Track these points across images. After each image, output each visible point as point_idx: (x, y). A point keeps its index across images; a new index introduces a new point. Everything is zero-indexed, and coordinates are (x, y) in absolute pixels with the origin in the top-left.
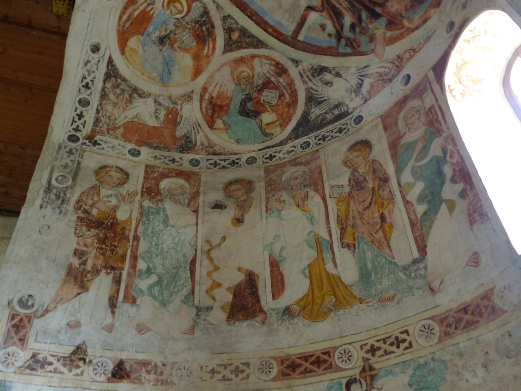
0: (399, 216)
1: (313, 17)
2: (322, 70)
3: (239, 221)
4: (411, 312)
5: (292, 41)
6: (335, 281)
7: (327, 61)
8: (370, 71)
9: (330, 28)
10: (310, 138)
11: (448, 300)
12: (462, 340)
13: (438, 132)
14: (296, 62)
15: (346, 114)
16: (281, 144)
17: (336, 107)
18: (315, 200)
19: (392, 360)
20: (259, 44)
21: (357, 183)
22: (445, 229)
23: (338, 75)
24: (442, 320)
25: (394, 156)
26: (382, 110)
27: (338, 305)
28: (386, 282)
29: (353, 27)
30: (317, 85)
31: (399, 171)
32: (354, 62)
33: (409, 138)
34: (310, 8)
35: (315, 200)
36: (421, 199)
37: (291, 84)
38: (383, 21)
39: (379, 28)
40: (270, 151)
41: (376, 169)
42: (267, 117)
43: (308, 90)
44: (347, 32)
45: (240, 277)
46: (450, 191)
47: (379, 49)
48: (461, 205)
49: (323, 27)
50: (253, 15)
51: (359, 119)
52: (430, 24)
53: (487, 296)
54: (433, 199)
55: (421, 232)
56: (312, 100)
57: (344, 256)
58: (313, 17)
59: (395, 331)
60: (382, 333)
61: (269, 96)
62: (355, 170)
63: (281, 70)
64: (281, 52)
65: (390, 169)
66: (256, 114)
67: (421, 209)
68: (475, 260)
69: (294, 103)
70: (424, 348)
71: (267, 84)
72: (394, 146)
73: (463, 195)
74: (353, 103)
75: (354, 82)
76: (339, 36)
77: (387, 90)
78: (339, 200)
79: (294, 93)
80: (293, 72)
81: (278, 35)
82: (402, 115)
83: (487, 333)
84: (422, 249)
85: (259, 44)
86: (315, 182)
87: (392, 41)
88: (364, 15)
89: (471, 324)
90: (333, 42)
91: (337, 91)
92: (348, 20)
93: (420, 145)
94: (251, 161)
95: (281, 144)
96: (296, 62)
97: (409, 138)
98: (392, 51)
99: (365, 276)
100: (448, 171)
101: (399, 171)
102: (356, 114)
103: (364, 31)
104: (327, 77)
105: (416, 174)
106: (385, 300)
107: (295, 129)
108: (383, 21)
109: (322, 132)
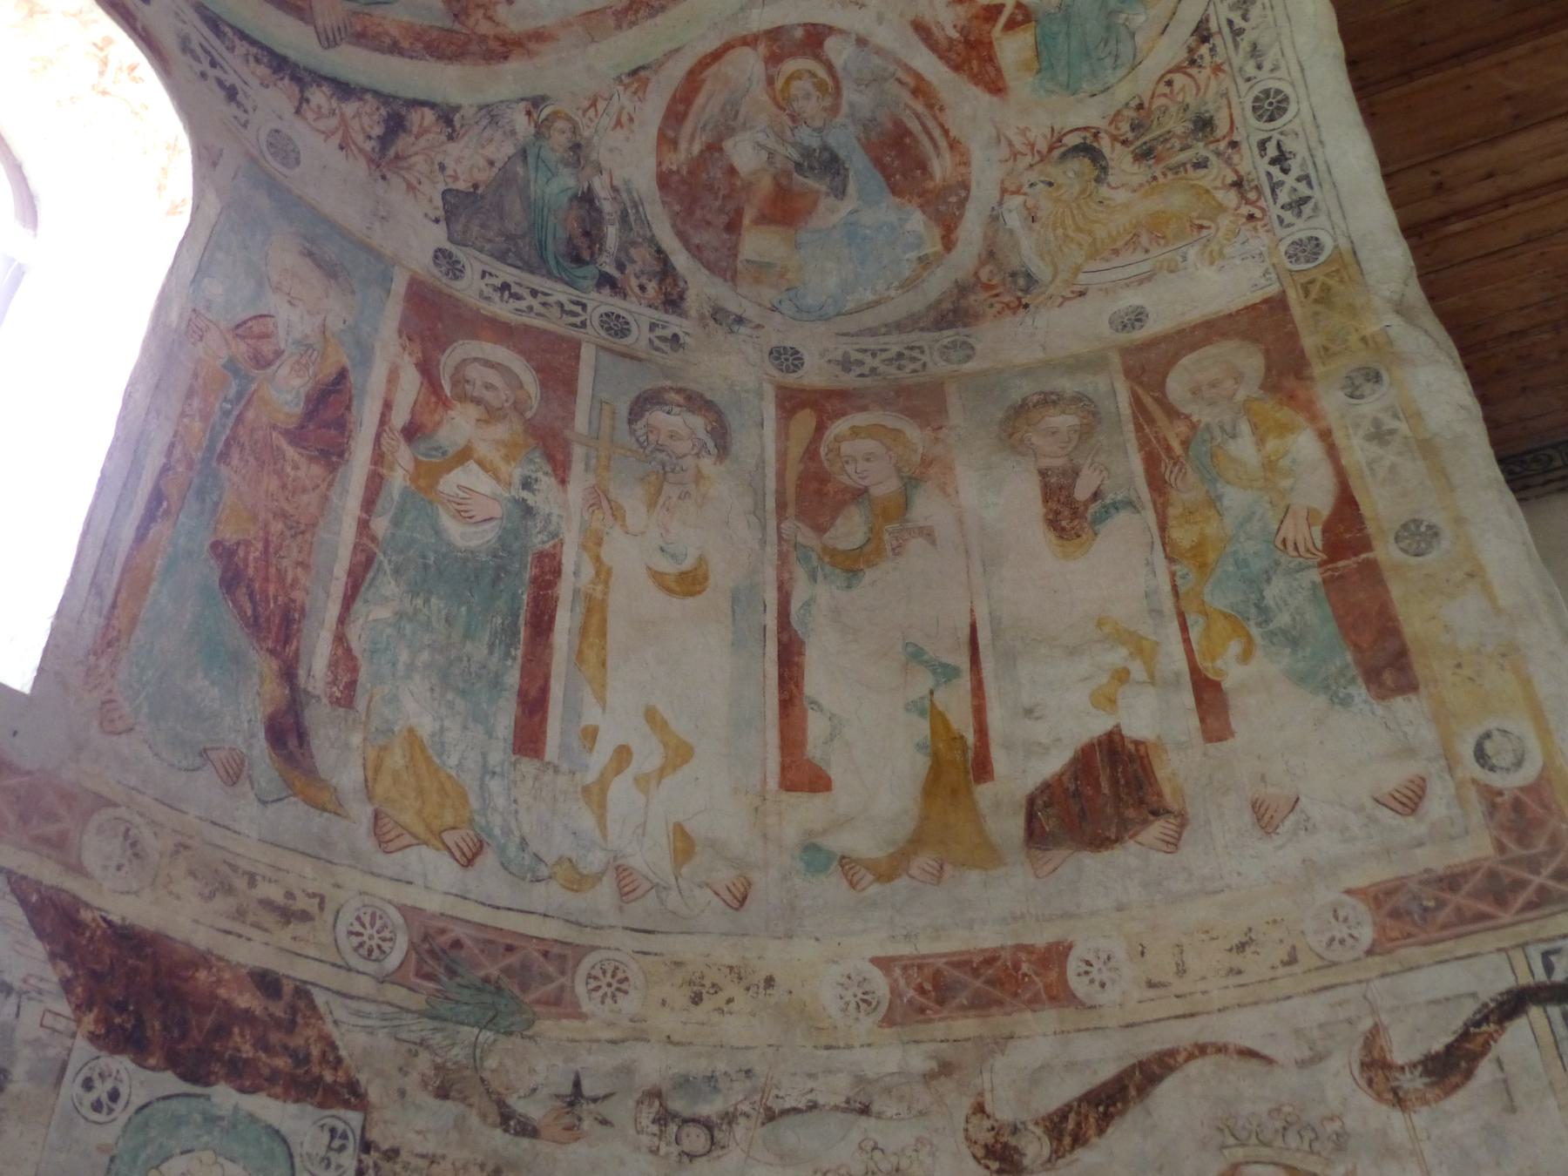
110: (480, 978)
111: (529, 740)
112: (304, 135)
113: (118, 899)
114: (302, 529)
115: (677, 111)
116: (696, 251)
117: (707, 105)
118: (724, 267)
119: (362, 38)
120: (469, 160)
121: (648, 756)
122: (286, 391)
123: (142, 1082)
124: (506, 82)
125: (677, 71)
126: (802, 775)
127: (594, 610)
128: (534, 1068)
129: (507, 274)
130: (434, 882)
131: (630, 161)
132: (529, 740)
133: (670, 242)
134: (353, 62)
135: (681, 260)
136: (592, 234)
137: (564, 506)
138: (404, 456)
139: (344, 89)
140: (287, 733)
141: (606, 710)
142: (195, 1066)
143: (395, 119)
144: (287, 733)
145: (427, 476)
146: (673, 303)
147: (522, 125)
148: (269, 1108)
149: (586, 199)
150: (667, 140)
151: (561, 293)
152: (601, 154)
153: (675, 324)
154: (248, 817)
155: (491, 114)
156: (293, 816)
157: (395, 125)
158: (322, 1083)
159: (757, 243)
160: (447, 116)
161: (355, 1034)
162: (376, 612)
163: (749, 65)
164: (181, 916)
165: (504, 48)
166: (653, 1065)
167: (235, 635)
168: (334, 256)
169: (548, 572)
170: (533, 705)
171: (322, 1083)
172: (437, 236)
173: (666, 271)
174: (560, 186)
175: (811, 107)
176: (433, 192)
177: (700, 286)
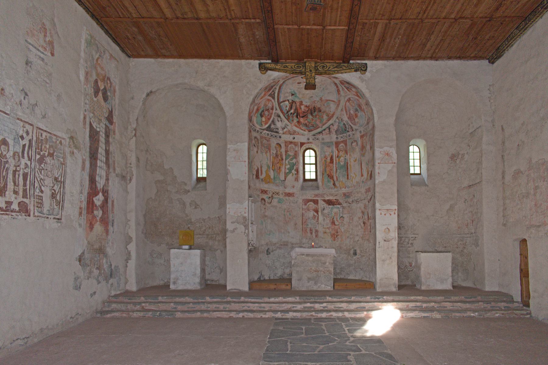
0: (283, 169)
1: (287, 103)
2: (279, 116)
3: (257, 152)
4: (280, 189)
5: (279, 103)
6: (270, 176)
7: (282, 115)
8: (288, 127)
9: (287, 108)
10: (269, 133)
11: (287, 191)
12: (287, 198)
13: (296, 158)
14: (276, 109)
15: (277, 132)
16: (264, 130)
17: (277, 129)
18: (268, 154)
19: (276, 196)
20: (274, 98)
21: (277, 155)
22: (290, 177)
23: (281, 121)
24: (285, 193)
25: (286, 155)
26: (286, 140)
27: (269, 182)
28: (278, 181)
29: (291, 113)
30: (276, 118)
31: (286, 159)
32: (286, 121)
33: (289, 153)
34: (288, 100)
35: (268, 154)
36: (288, 169)
37: (272, 114)
38: (297, 120)
39: (296, 120)
40: (261, 131)
41: (281, 155)
42: (264, 119)
43: (274, 118)
44: (289, 113)
45: (256, 168)
46: (293, 171)
47: (293, 124)
48: (294, 176)
49: (286, 107)
50: (279, 92)
51: (280, 137)
52: (305, 132)
53: (293, 193)
54: (290, 170)
55: (286, 175)
56: (273, 121)
57: (272, 171)
58: (287, 103)
59: (277, 191)
60: (275, 191)
61: (266, 113)
62: (277, 151)
63: (272, 109)
64: (276, 104)
65: (284, 158)
66: (262, 116)
67: (287, 171)
68: (294, 187)
69: (269, 119)
70: (281, 197)
71: (268, 110)
72: (286, 152)
73: (296, 174)
74: (281, 131)
75: (283, 126)
76: (288, 112)
77: (289, 135)
78: (273, 157)
79: (271, 117)
80: (274, 111)
81: (278, 100)
82: (290, 146)
83: (291, 198)
84: (285, 179)
85: (274, 98)
86: (269, 148)
87: (296, 126)
88: (295, 114)
89: (289, 196)
90: (286, 112)
91: (279, 125)
92: (292, 111)
93: (291, 157)
94: (258, 131)
95: (264, 130)
96: (276, 109)
97: (289, 153)
98: (295, 128)
99: (274, 178)
100: (295, 168)
101: (286, 159)
102: (280, 135)
103: (293, 117)
104: (279, 119)
105: (289, 163)
106: (277, 185)
107: (267, 128)
108: (297, 120)
109: (273, 133)
110: (346, 195)
111: (348, 178)
112: (324, 136)
113: (327, 198)
114: (331, 170)
115: (346, 112)
116: (352, 123)
117: (347, 109)
118: (355, 124)
119: (324, 125)
120: (335, 127)
121: (354, 176)
122: (329, 160)
123: (331, 206)
124: (335, 118)
125: (344, 107)
126: (362, 176)
127: (350, 165)
128: (350, 200)
129: (341, 135)
130: (344, 190)
131: (345, 118)
132: (348, 178)
133: (351, 124)
134: (324, 127)
135: (352, 125)
136: (346, 127)
137: (348, 157)
138: (337, 159)
139: (325, 130)
140: (334, 184)
141: (351, 174)
142: (333, 205)
143: (329, 128)
144: (334, 184)
145: (339, 160)
146: (353, 130)
147: (337, 120)
148: (338, 206)
149: (344, 124)
150: (347, 114)
151: (345, 135)
152: (344, 119)
153: (353, 132)
154: (333, 190)
155: (335, 121)
156: (336, 189)
157: (329, 129)
158: (340, 204)
159: (356, 120)
160: (332, 124)
161: (341, 201)
162: (338, 173)
163: (348, 103)
164: (331, 198)
165: (333, 115)
166: (356, 198)
167: (330, 180)
168: (329, 144)
169: (347, 163)
170: (348, 175)
171: (340, 204)
172: (336, 136)
173: (352, 127)
174: (342, 125)
175: (353, 105)
176: (334, 133)
177: (354, 127)
